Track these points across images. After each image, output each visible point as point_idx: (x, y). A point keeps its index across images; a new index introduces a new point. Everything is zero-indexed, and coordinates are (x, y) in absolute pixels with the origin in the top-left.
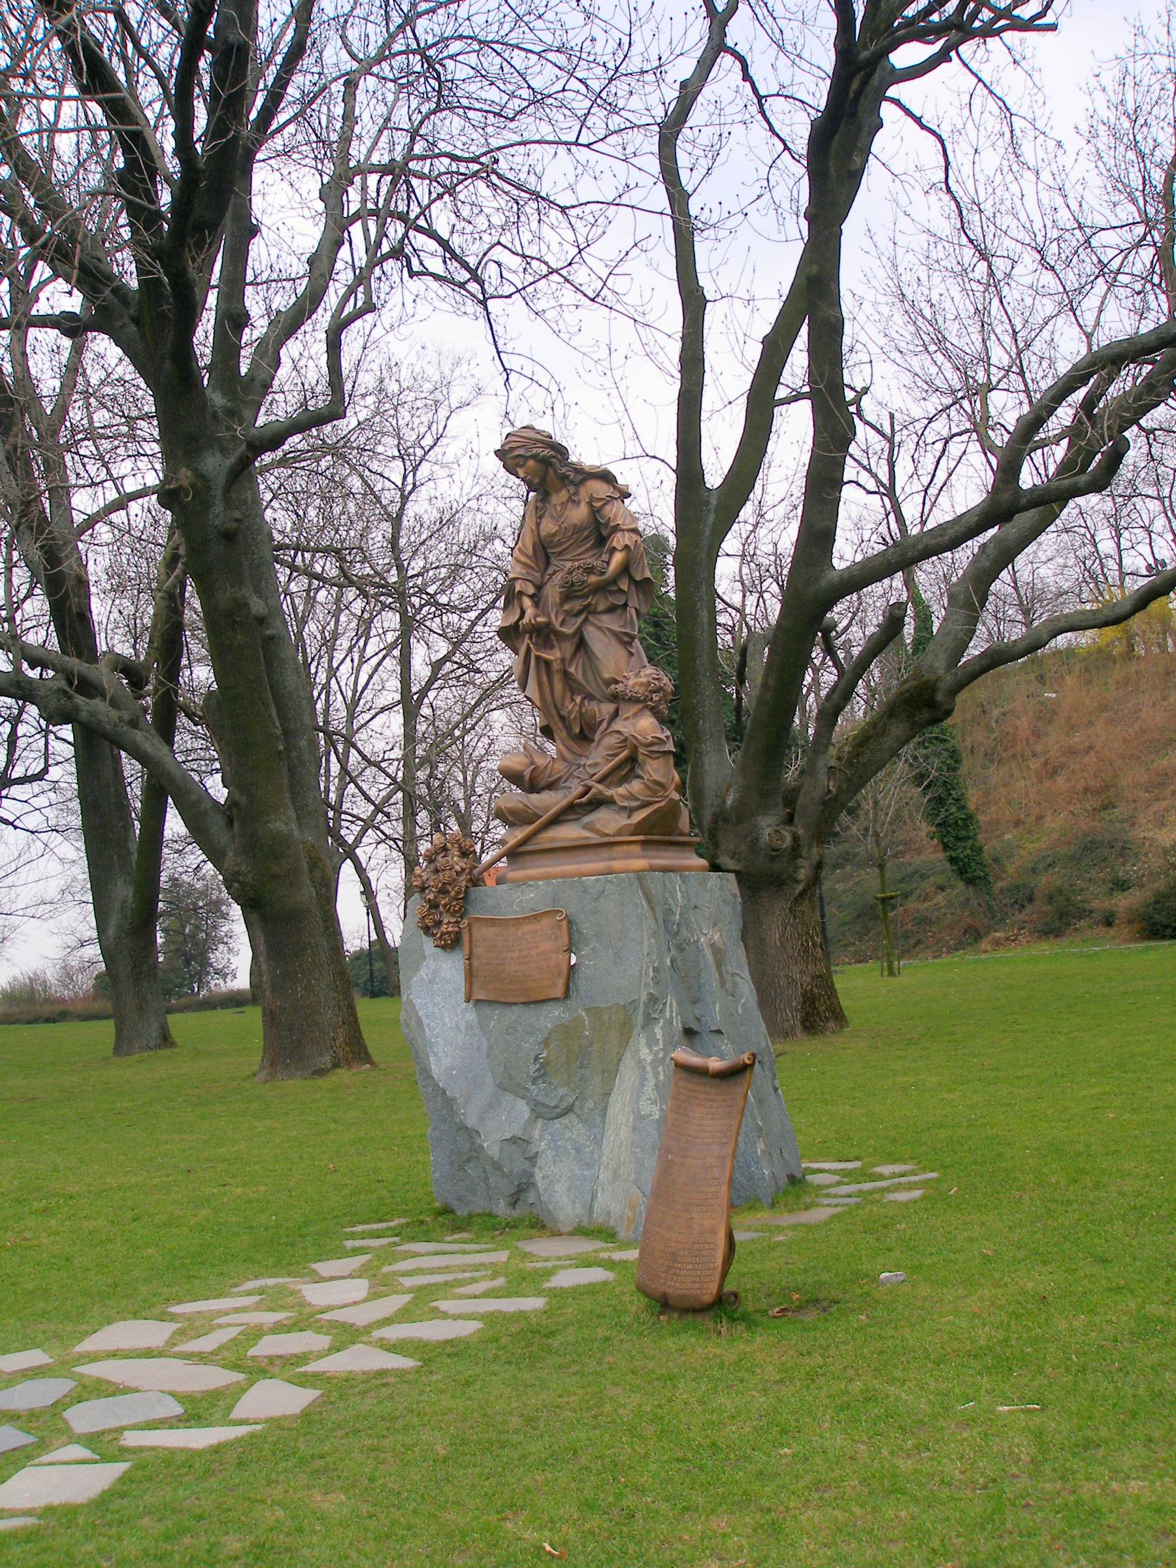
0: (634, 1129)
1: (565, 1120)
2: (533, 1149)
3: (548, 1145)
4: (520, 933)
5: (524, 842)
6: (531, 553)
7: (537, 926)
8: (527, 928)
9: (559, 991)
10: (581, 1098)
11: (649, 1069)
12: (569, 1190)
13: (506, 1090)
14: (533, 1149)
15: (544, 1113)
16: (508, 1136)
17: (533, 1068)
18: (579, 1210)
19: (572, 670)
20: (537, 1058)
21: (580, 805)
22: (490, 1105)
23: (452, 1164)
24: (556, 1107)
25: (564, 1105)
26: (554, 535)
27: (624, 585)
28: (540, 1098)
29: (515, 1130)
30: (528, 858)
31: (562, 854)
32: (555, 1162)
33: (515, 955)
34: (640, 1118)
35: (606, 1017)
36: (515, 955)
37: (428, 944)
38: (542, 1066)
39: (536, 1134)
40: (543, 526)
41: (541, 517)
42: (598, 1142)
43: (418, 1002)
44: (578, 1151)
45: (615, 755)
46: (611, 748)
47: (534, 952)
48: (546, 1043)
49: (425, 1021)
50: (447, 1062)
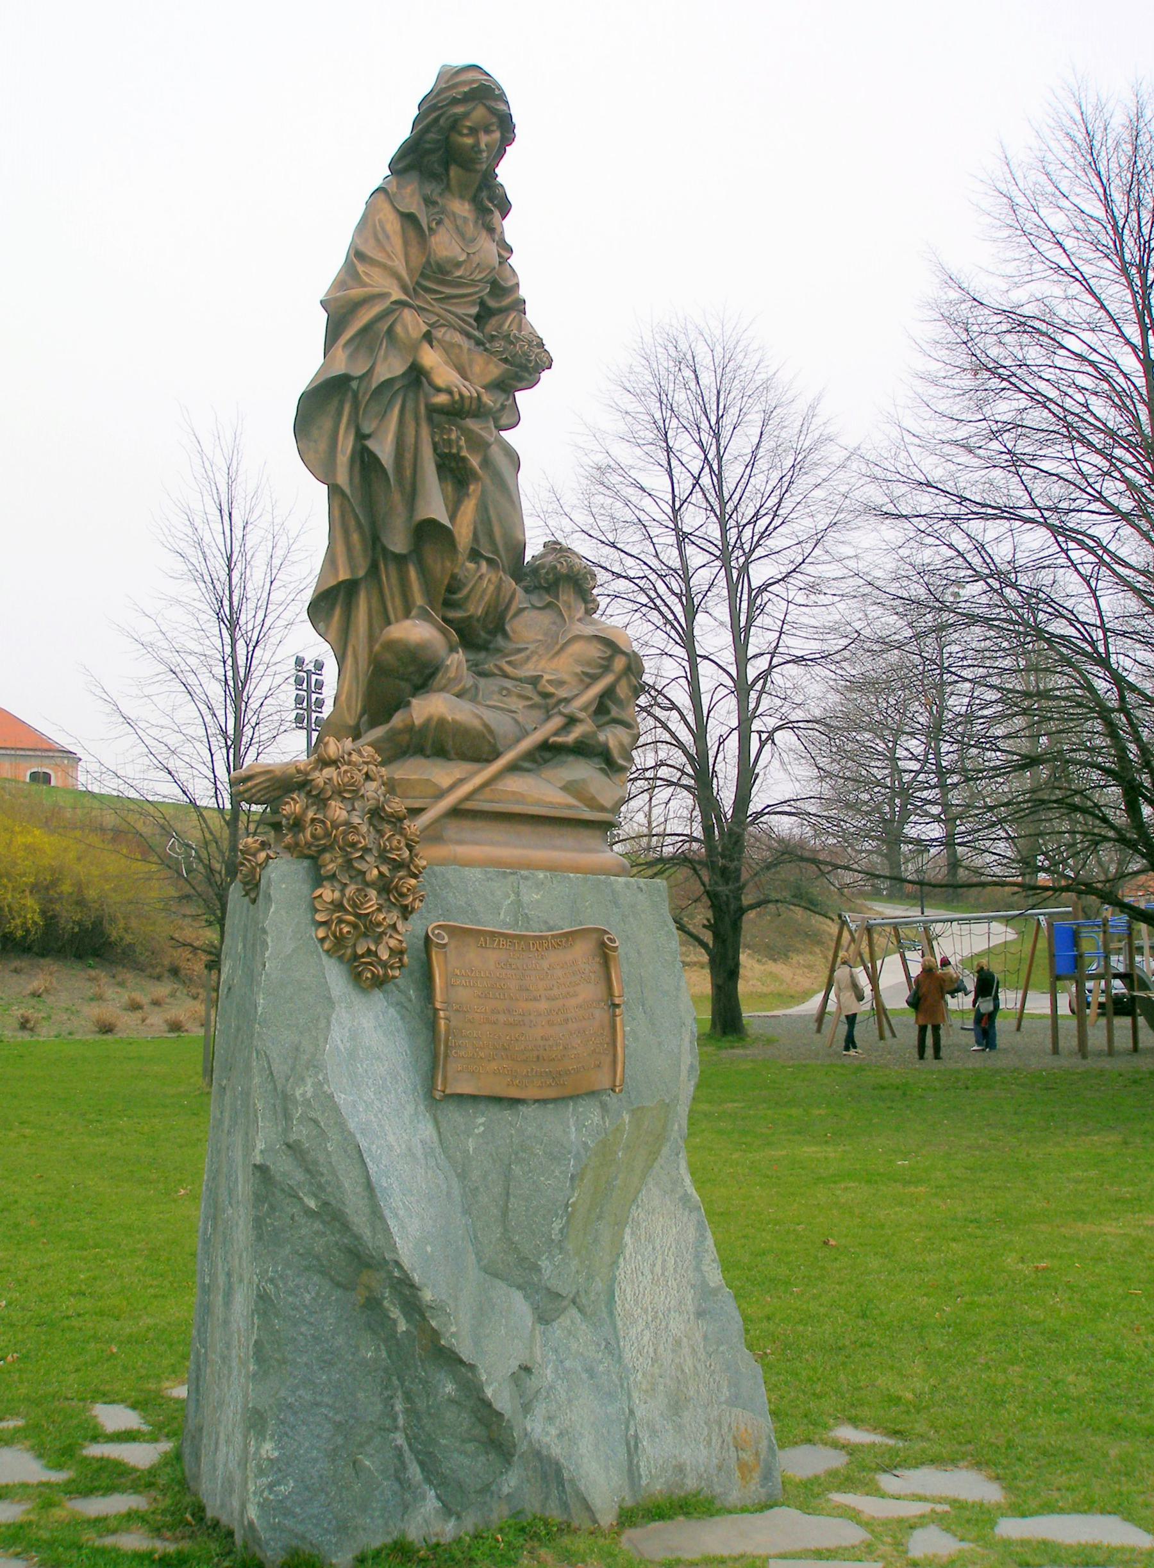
0: (700, 1314)
4: (545, 964)
13: (496, 1275)
23: (333, 1455)
26: (458, 265)
31: (525, 829)
33: (543, 1005)
34: (705, 1292)
36: (543, 1005)
41: (439, 223)
42: (612, 1348)
43: (341, 1098)
44: (591, 1372)
45: (594, 678)
46: (588, 664)
47: (572, 1002)
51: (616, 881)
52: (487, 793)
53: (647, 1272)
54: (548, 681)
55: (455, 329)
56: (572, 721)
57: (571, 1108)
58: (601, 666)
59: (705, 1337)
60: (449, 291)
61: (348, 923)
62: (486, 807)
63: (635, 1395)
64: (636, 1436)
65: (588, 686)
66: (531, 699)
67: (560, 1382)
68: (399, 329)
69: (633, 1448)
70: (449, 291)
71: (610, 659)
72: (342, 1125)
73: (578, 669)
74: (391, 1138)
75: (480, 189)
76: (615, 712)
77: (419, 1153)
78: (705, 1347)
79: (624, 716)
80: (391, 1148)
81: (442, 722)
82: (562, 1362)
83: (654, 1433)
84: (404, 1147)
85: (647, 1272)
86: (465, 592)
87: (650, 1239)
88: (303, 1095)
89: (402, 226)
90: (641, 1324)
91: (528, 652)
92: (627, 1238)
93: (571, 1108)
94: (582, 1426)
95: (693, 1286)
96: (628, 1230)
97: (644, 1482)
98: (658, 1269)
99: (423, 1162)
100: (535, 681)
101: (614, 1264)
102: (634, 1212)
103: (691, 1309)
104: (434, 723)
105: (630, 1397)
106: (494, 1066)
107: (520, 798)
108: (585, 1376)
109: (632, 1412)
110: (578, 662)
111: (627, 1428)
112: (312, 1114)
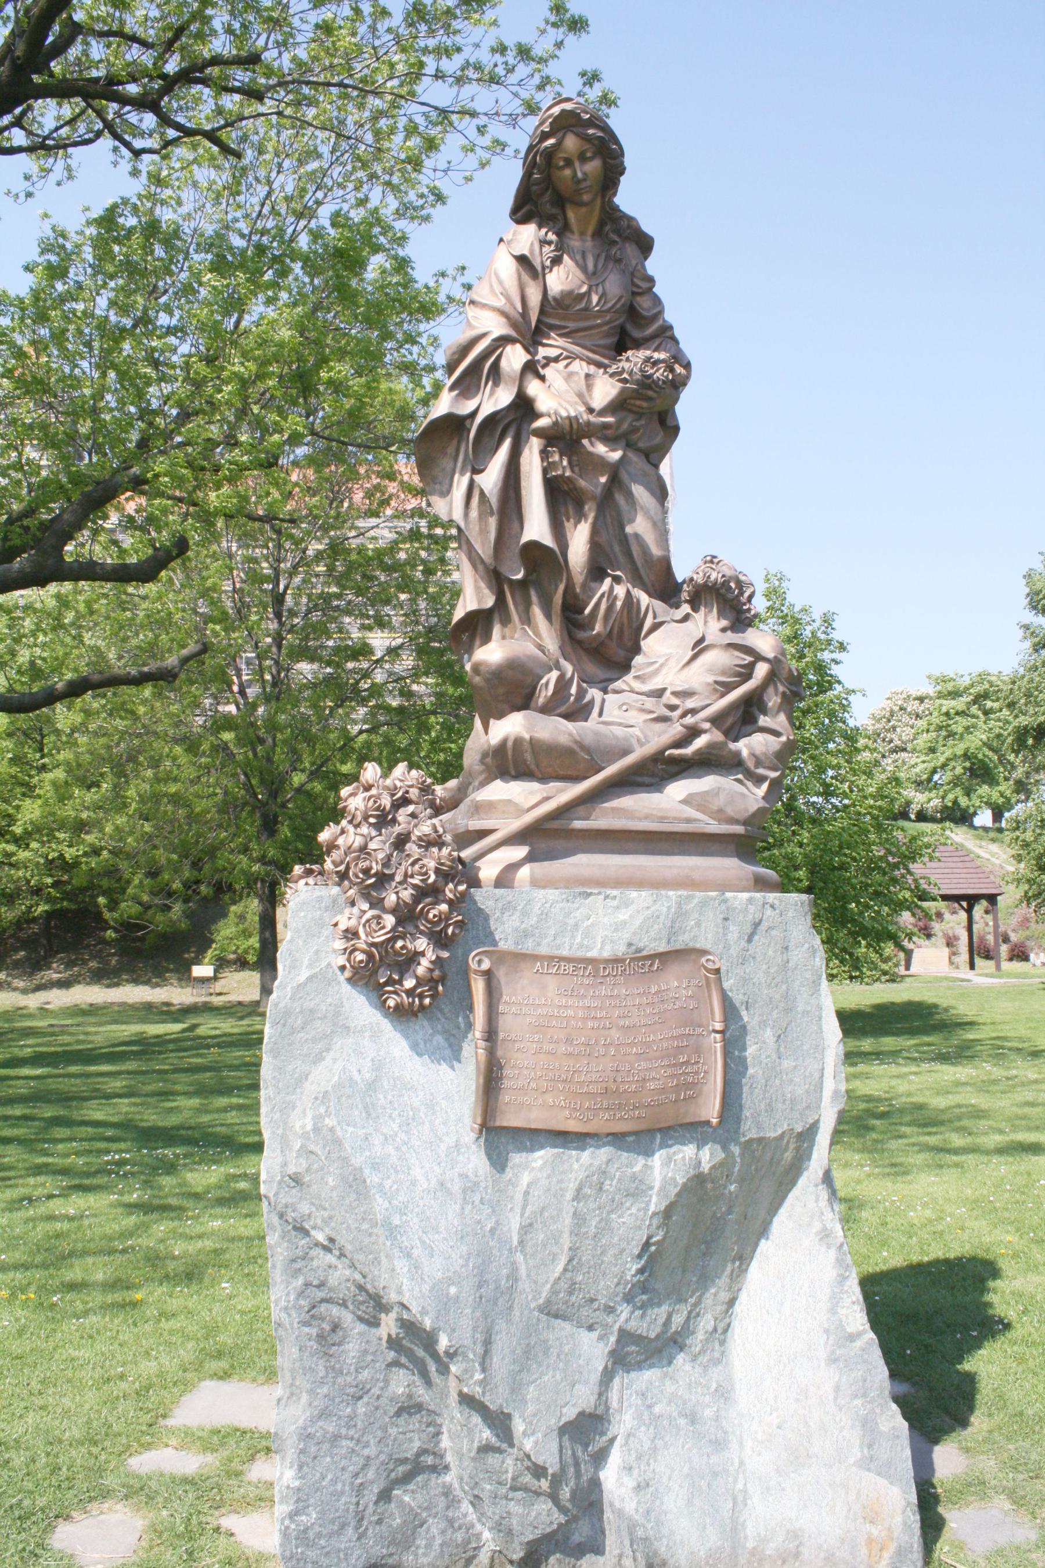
0: (832, 1360)
3: (639, 1417)
9: (711, 1109)
12: (690, 1502)
13: (556, 1316)
15: (632, 1353)
16: (570, 1413)
20: (647, 1244)
21: (674, 761)
22: (527, 1352)
29: (582, 1398)
30: (559, 844)
37: (359, 1006)
38: (652, 1259)
45: (729, 687)
46: (724, 673)
49: (373, 1178)
50: (435, 1268)
51: (735, 898)
54: (675, 694)
55: (582, 359)
56: (694, 732)
57: (658, 1141)
58: (738, 674)
59: (837, 1389)
61: (363, 951)
64: (745, 1491)
65: (723, 695)
66: (652, 712)
67: (643, 1429)
68: (503, 363)
71: (751, 667)
72: (345, 1160)
73: (711, 679)
75: (601, 224)
77: (456, 1187)
78: (835, 1399)
80: (414, 1183)
81: (518, 742)
82: (650, 1407)
84: (434, 1181)
86: (587, 611)
88: (303, 1127)
89: (518, 270)
91: (657, 666)
93: (658, 1141)
94: (670, 1478)
100: (659, 693)
104: (510, 744)
107: (618, 812)
108: (682, 1422)
109: (742, 1463)
110: (710, 671)
111: (735, 1481)
112: (312, 1147)
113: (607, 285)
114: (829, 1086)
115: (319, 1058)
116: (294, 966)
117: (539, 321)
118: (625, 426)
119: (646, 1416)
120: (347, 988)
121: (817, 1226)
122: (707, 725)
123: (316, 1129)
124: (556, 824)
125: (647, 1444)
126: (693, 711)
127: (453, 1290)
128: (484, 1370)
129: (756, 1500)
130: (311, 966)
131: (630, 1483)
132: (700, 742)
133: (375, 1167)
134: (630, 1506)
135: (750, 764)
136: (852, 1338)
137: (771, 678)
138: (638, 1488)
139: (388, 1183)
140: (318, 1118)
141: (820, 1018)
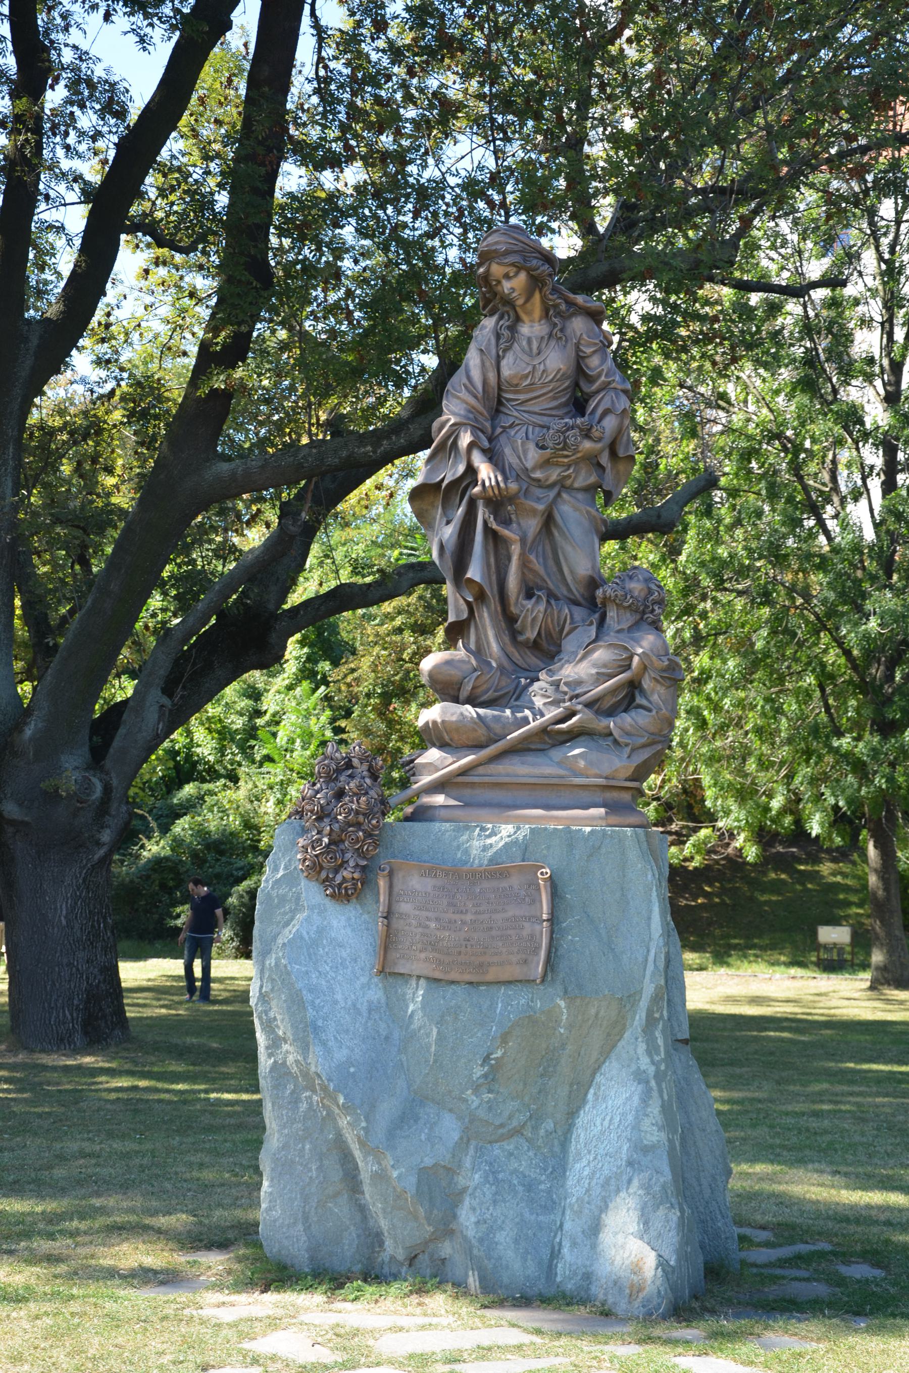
1: (509, 1146)
2: (461, 1181)
5: (464, 772)
6: (480, 395)
7: (504, 884)
8: (486, 885)
10: (536, 1118)
11: (653, 1083)
12: (516, 1241)
14: (461, 1181)
16: (428, 1162)
17: (479, 1072)
18: (532, 1269)
19: (532, 557)
24: (502, 1126)
25: (515, 1123)
27: (604, 460)
28: (482, 1114)
32: (495, 1202)
33: (468, 917)
35: (593, 1011)
36: (468, 917)
39: (468, 1162)
40: (504, 363)
41: (505, 351)
44: (530, 1187)
46: (605, 666)
48: (504, 1038)
49: (307, 996)
52: (481, 770)
53: (598, 1123)
54: (566, 684)
60: (522, 397)
62: (476, 779)
63: (568, 1212)
64: (560, 1244)
69: (555, 1254)
70: (522, 397)
73: (594, 671)
74: (339, 997)
76: (640, 700)
77: (364, 1009)
79: (644, 702)
80: (336, 1002)
81: (435, 723)
83: (574, 1244)
85: (598, 1123)
87: (604, 1099)
90: (584, 1162)
92: (590, 1096)
95: (629, 1140)
96: (592, 1091)
97: (559, 1279)
98: (606, 1123)
99: (365, 1014)
101: (572, 1114)
102: (598, 1078)
103: (624, 1157)
105: (563, 1213)
106: (423, 955)
108: (520, 1188)
109: (561, 1226)
110: (594, 665)
113: (548, 362)
114: (650, 967)
115: (287, 924)
116: (276, 869)
117: (499, 396)
118: (554, 477)
119: (491, 1179)
120: (303, 883)
121: (634, 1067)
122: (579, 707)
123: (277, 965)
124: (461, 779)
125: (489, 1195)
126: (577, 696)
127: (352, 1070)
128: (367, 1120)
129: (565, 1251)
130: (286, 868)
131: (473, 1219)
132: (574, 719)
133: (310, 991)
134: (471, 1233)
135: (616, 733)
136: (646, 1150)
137: (645, 668)
138: (478, 1223)
139: (317, 1001)
140: (278, 960)
141: (649, 918)
